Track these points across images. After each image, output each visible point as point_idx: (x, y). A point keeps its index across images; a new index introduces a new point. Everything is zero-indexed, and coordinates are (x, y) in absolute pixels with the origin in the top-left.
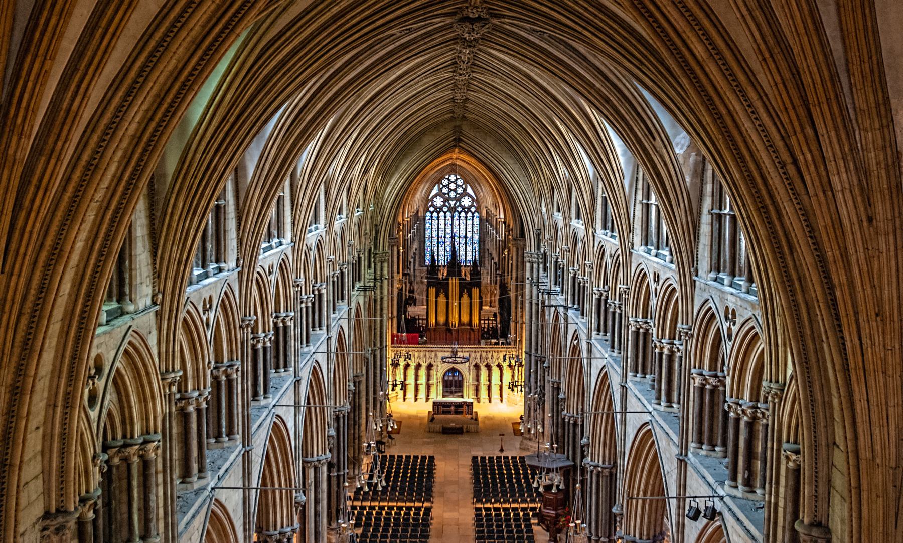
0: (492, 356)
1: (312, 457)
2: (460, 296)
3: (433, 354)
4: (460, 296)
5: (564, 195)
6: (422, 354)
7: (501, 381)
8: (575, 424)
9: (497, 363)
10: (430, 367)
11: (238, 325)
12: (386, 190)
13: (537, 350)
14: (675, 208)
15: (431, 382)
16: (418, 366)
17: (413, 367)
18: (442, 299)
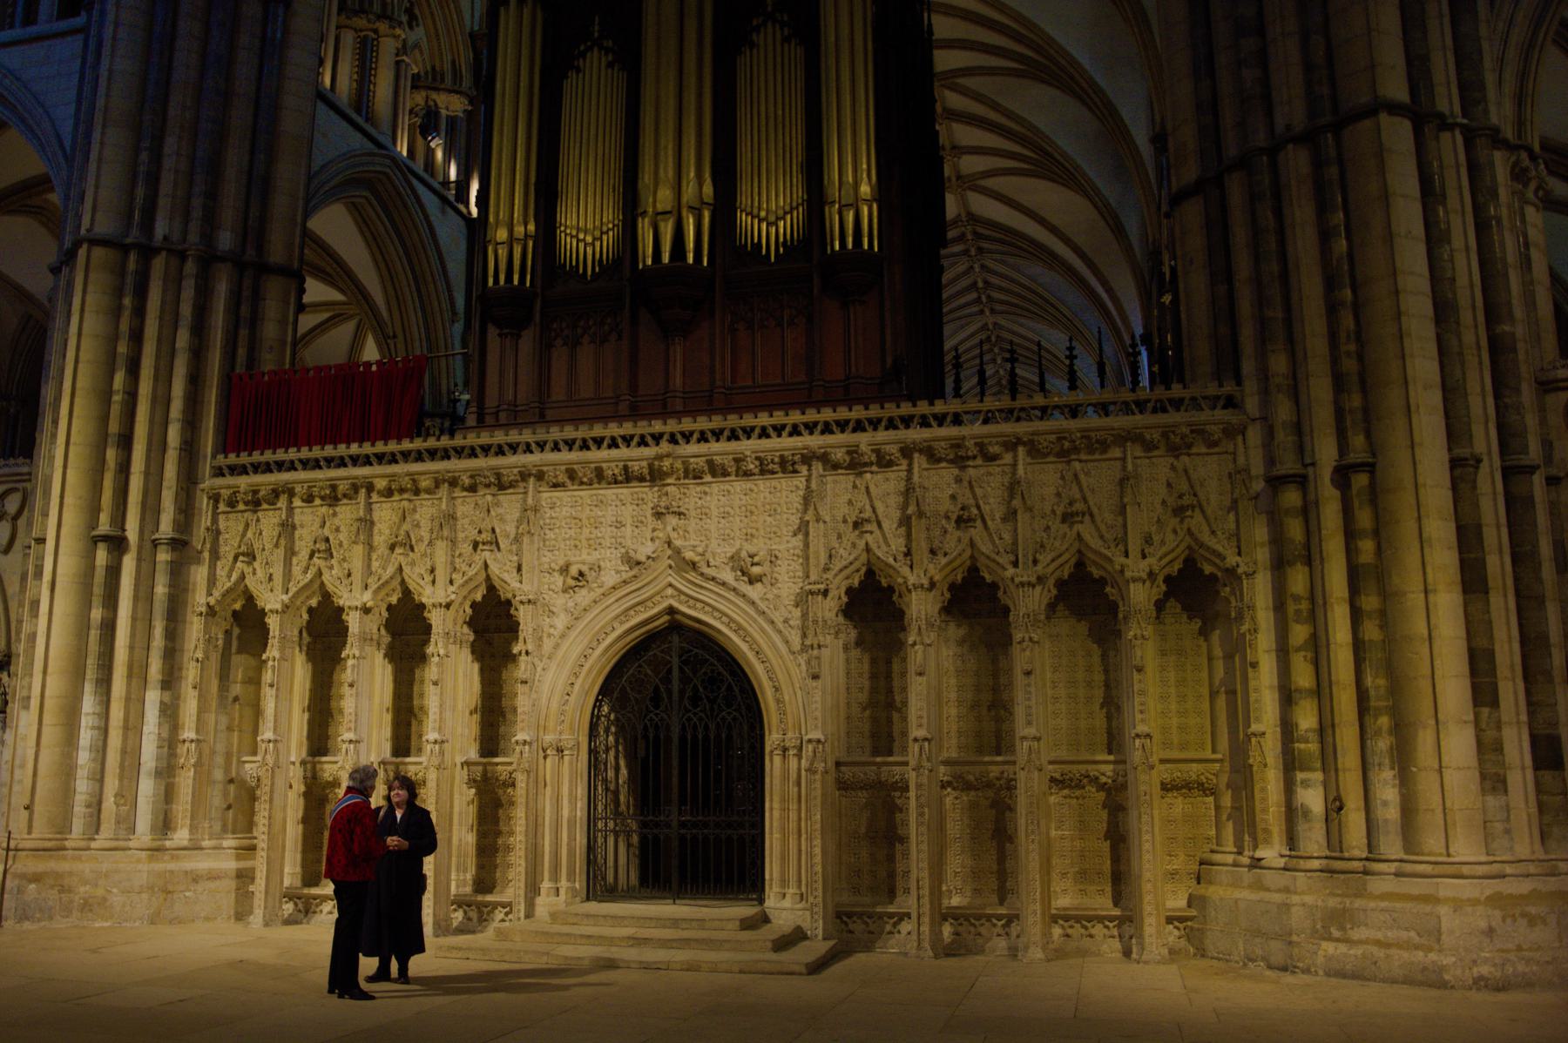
3: (509, 506)
6: (426, 511)
15: (502, 764)
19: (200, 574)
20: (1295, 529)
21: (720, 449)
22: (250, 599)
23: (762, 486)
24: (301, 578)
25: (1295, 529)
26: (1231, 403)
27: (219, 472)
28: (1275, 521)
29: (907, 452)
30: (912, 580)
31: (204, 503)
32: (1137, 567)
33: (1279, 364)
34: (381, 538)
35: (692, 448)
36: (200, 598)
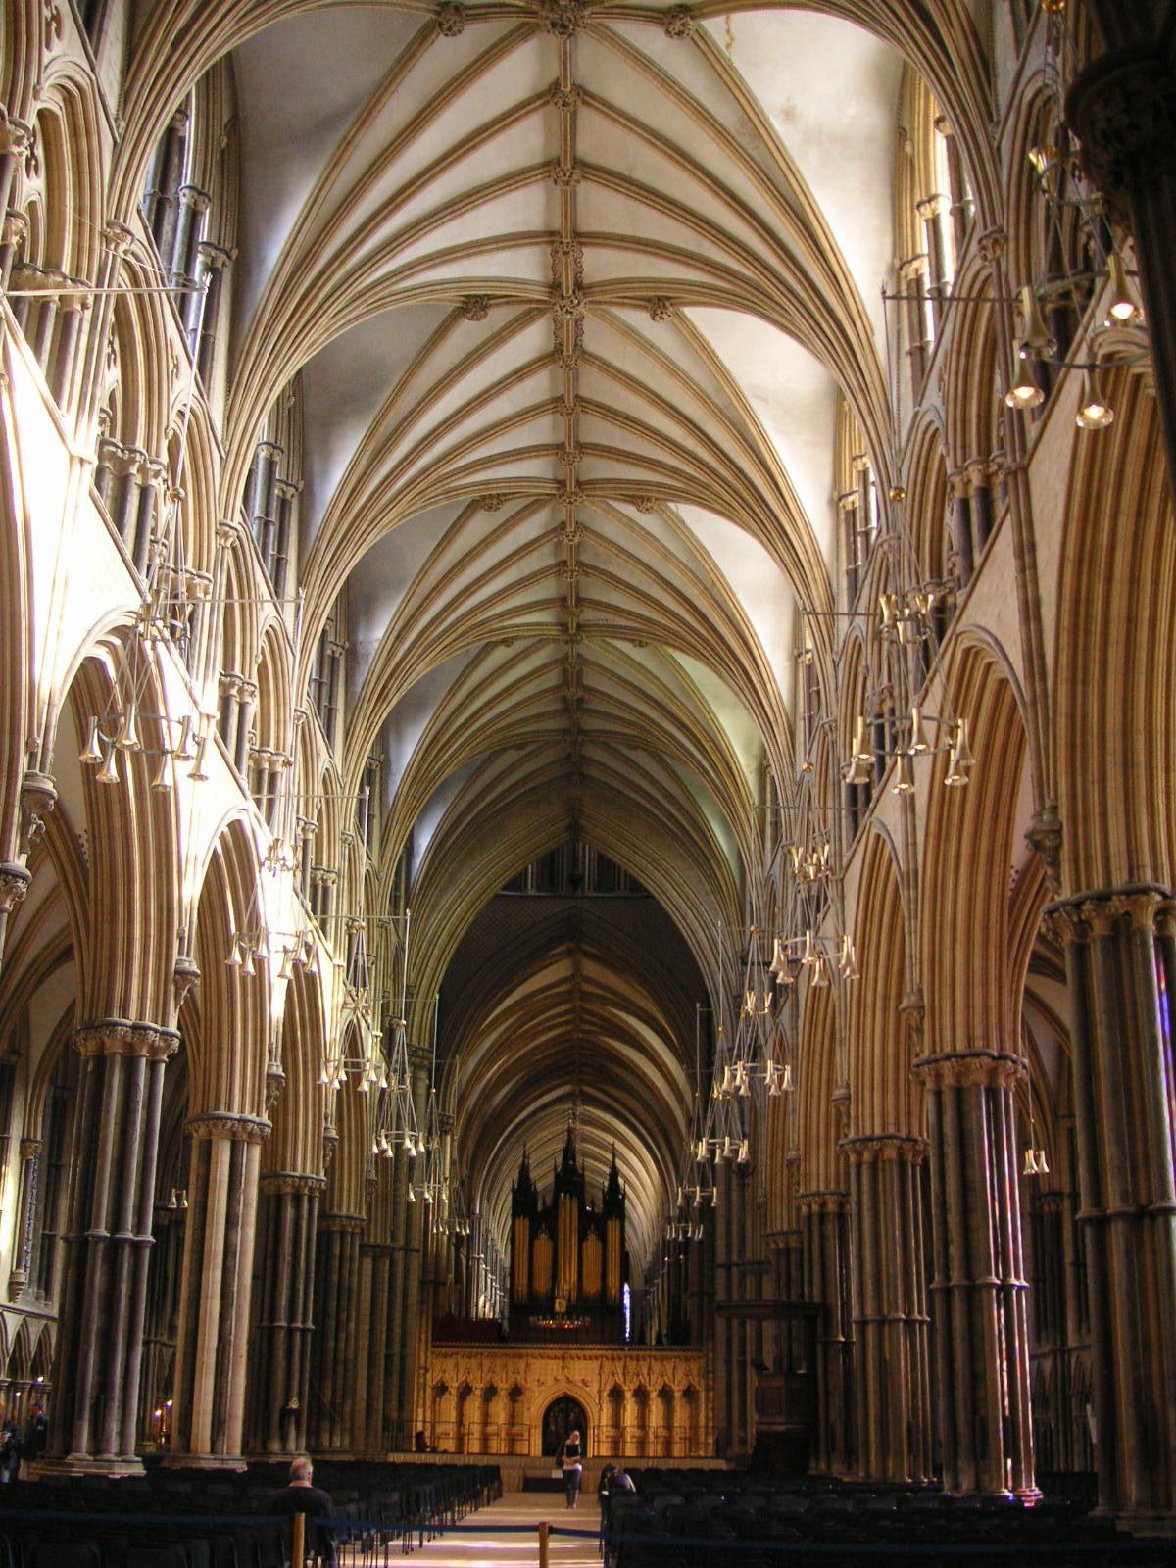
0: (650, 1368)
1: (230, 1109)
2: (582, 1238)
3: (522, 1364)
4: (582, 1238)
5: (781, 738)
6: (499, 1362)
7: (669, 1426)
8: (823, 1217)
9: (659, 1386)
10: (516, 1392)
11: (98, 229)
12: (428, 918)
13: (742, 1252)
14: (942, 31)
16: (490, 1392)
17: (478, 1392)
18: (543, 1243)
19: (429, 1375)
20: (711, 1383)
21: (579, 1352)
22: (443, 1383)
23: (589, 1363)
24: (462, 1378)
25: (711, 1383)
26: (700, 1351)
27: (434, 1347)
28: (707, 1380)
29: (626, 1357)
30: (625, 1388)
31: (429, 1355)
32: (675, 1388)
33: (711, 1345)
34: (486, 1368)
35: (573, 1353)
36: (429, 1383)
